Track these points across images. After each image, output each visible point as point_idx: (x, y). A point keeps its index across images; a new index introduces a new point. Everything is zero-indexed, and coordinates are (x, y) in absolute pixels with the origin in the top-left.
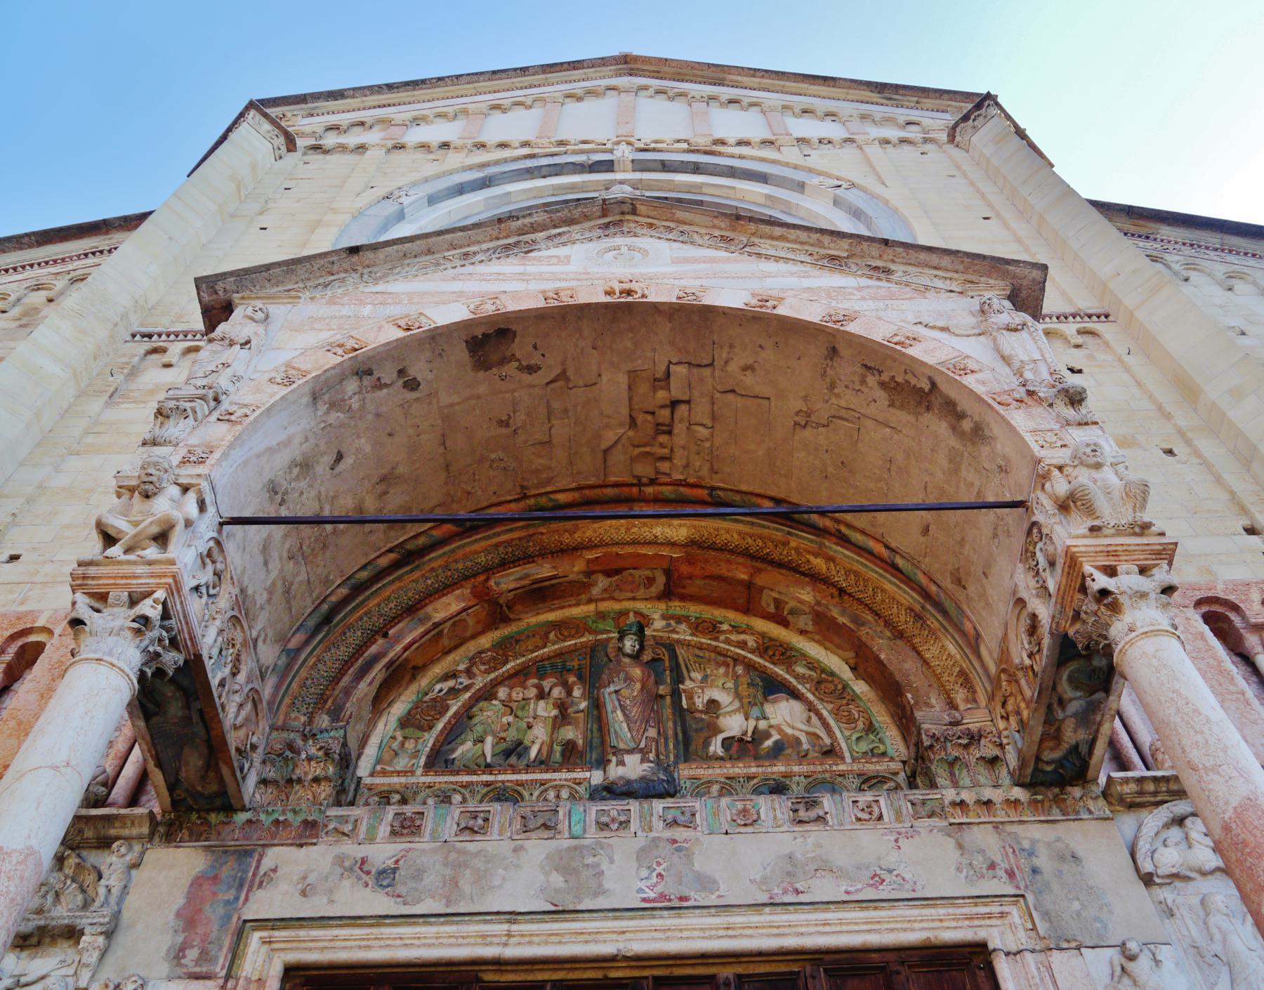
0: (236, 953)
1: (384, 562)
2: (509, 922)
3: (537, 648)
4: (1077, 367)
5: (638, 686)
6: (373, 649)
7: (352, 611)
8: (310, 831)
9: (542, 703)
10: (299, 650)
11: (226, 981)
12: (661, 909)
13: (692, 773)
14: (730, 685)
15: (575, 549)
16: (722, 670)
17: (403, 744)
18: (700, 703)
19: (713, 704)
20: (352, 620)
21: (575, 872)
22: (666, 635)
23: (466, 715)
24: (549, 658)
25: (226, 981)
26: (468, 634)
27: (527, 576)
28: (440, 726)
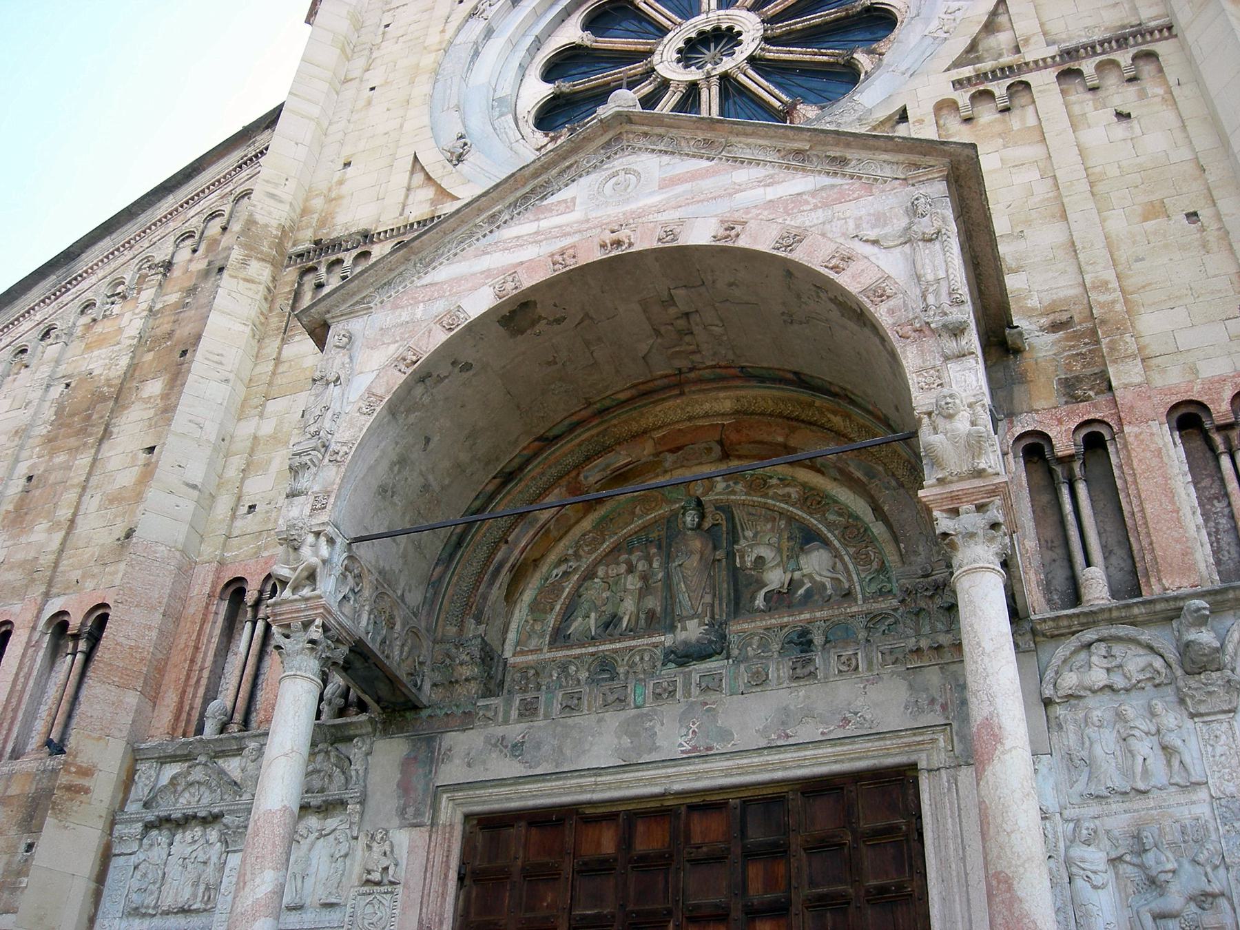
0: (435, 808)
1: (491, 488)
2: (595, 775)
3: (628, 524)
4: (1125, 110)
6: (499, 556)
7: (476, 531)
8: (467, 720)
9: (630, 577)
10: (441, 578)
11: (432, 827)
12: (694, 757)
13: (739, 627)
14: (774, 540)
15: (645, 432)
16: (769, 526)
17: (533, 625)
19: (760, 560)
20: (478, 537)
21: (637, 734)
22: (726, 497)
23: (576, 595)
24: (636, 533)
25: (432, 827)
26: (572, 521)
27: (608, 466)
28: (558, 608)
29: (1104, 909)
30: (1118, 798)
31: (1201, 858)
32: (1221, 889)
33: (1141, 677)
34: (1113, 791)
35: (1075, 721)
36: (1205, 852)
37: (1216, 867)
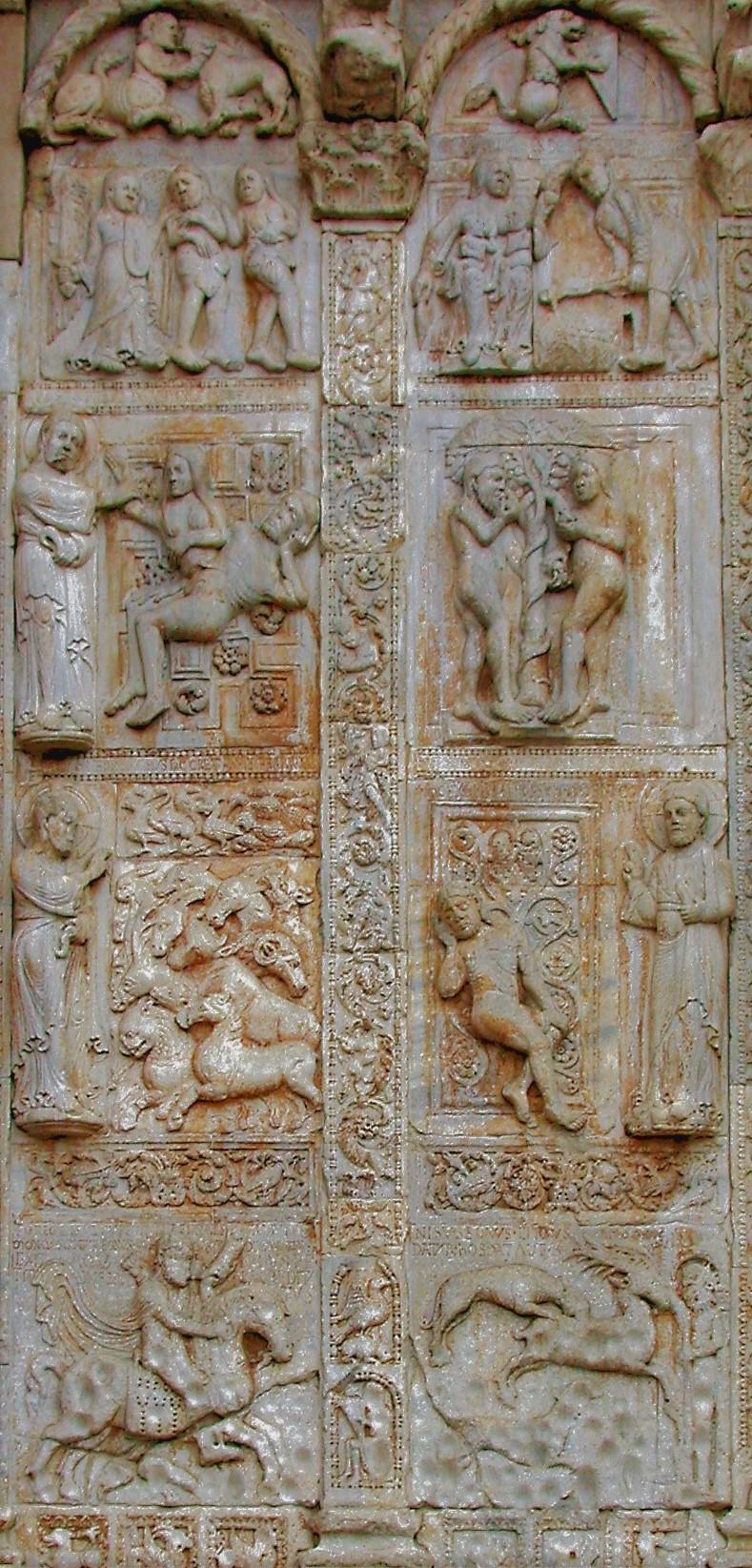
29: (73, 610)
30: (140, 377)
31: (276, 527)
32: (303, 596)
33: (233, 108)
34: (132, 362)
35: (82, 193)
36: (286, 516)
37: (300, 550)
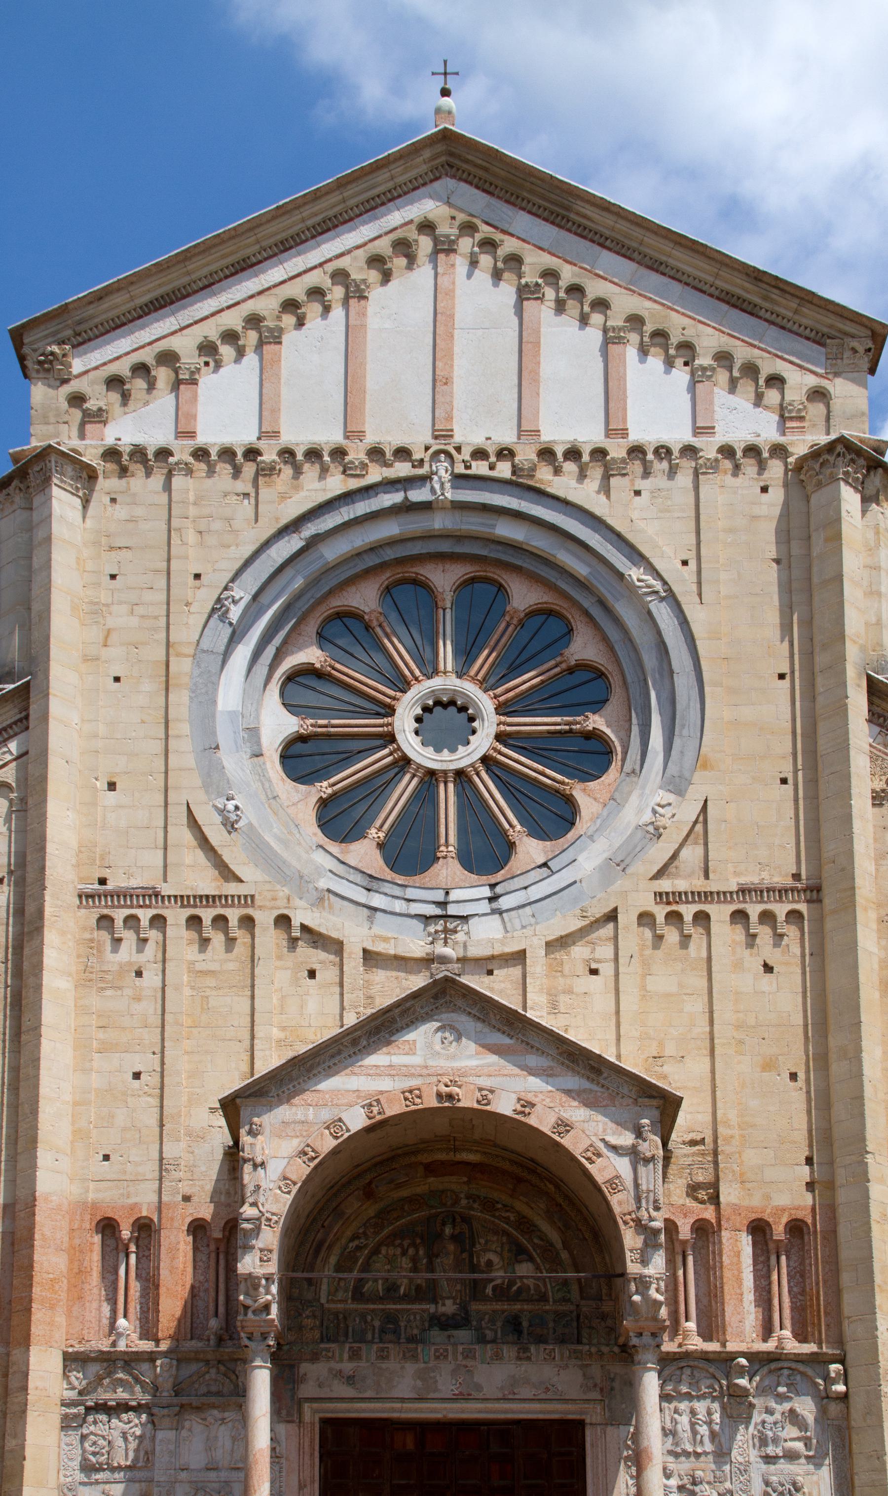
5: (452, 1257)
9: (404, 1259)
14: (499, 1249)
16: (495, 1238)
18: (483, 1261)
